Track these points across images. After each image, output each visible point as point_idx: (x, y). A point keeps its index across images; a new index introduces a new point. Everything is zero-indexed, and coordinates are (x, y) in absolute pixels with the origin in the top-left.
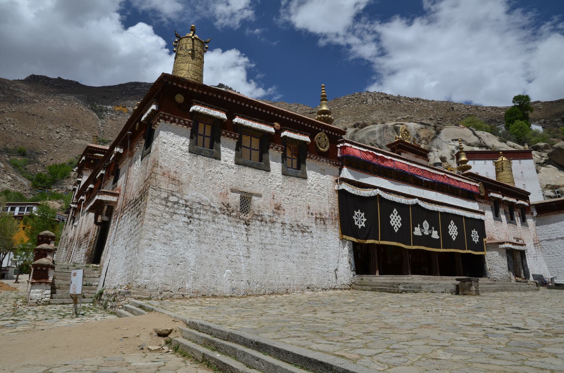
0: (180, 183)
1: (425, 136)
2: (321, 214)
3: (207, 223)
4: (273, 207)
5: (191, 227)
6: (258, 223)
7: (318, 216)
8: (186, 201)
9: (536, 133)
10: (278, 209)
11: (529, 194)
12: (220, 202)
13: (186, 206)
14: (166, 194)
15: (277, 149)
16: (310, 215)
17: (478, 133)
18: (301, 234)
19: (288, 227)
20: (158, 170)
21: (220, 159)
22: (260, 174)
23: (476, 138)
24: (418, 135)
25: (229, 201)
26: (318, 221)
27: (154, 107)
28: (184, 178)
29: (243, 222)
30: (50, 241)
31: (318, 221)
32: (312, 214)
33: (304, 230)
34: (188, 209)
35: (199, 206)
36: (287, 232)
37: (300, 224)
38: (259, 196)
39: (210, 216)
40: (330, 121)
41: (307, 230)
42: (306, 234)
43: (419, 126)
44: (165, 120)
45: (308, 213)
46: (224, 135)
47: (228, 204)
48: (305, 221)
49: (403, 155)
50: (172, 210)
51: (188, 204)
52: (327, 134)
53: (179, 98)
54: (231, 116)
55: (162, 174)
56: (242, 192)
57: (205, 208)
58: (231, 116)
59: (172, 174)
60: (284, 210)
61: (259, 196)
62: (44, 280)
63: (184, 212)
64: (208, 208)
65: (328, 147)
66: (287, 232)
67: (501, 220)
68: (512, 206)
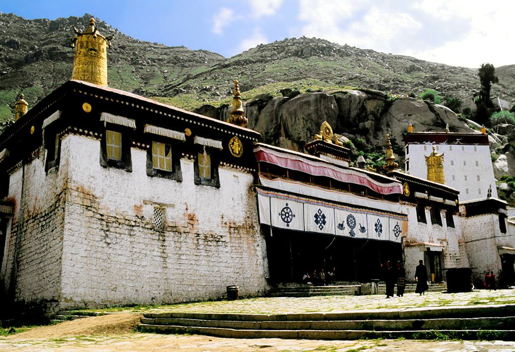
1: (372, 109)
2: (234, 224)
4: (187, 218)
6: (172, 234)
7: (232, 225)
8: (102, 215)
10: (192, 220)
11: (458, 193)
13: (103, 220)
15: (189, 158)
16: (224, 225)
18: (215, 243)
19: (202, 236)
20: (71, 185)
24: (363, 108)
25: (143, 214)
26: (232, 230)
28: (98, 194)
29: (158, 233)
31: (232, 230)
32: (226, 224)
33: (217, 240)
34: (104, 223)
36: (201, 242)
38: (173, 206)
39: (124, 229)
41: (221, 239)
42: (220, 243)
43: (364, 95)
44: (75, 133)
46: (135, 146)
48: (220, 231)
51: (103, 218)
52: (240, 138)
53: (87, 107)
54: (141, 125)
55: (76, 189)
56: (156, 203)
57: (120, 221)
58: (141, 125)
60: (197, 220)
61: (173, 206)
65: (241, 153)
66: (201, 242)
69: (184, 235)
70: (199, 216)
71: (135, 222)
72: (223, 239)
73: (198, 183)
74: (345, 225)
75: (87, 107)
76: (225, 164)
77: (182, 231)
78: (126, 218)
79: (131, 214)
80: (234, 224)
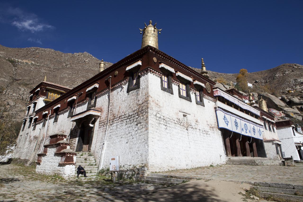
0: (160, 107)
3: (173, 129)
5: (167, 131)
7: (211, 126)
9: (250, 88)
12: (176, 118)
14: (155, 113)
17: (226, 86)
21: (173, 95)
22: (188, 102)
23: (225, 88)
26: (211, 128)
27: (140, 63)
30: (64, 138)
31: (211, 128)
34: (165, 121)
35: (169, 120)
36: (201, 134)
37: (205, 130)
40: (208, 77)
42: (208, 135)
45: (207, 124)
47: (179, 119)
49: (234, 96)
50: (158, 122)
51: (164, 118)
53: (155, 59)
59: (156, 102)
62: (71, 162)
63: (163, 123)
64: (172, 121)
65: (210, 91)
67: (267, 130)
68: (269, 122)
69: (195, 130)
70: (199, 121)
71: (177, 121)
72: (208, 133)
73: (197, 103)
74: (244, 129)
75: (155, 59)
76: (206, 95)
77: (194, 127)
78: (173, 119)
79: (175, 117)
80: (211, 125)
